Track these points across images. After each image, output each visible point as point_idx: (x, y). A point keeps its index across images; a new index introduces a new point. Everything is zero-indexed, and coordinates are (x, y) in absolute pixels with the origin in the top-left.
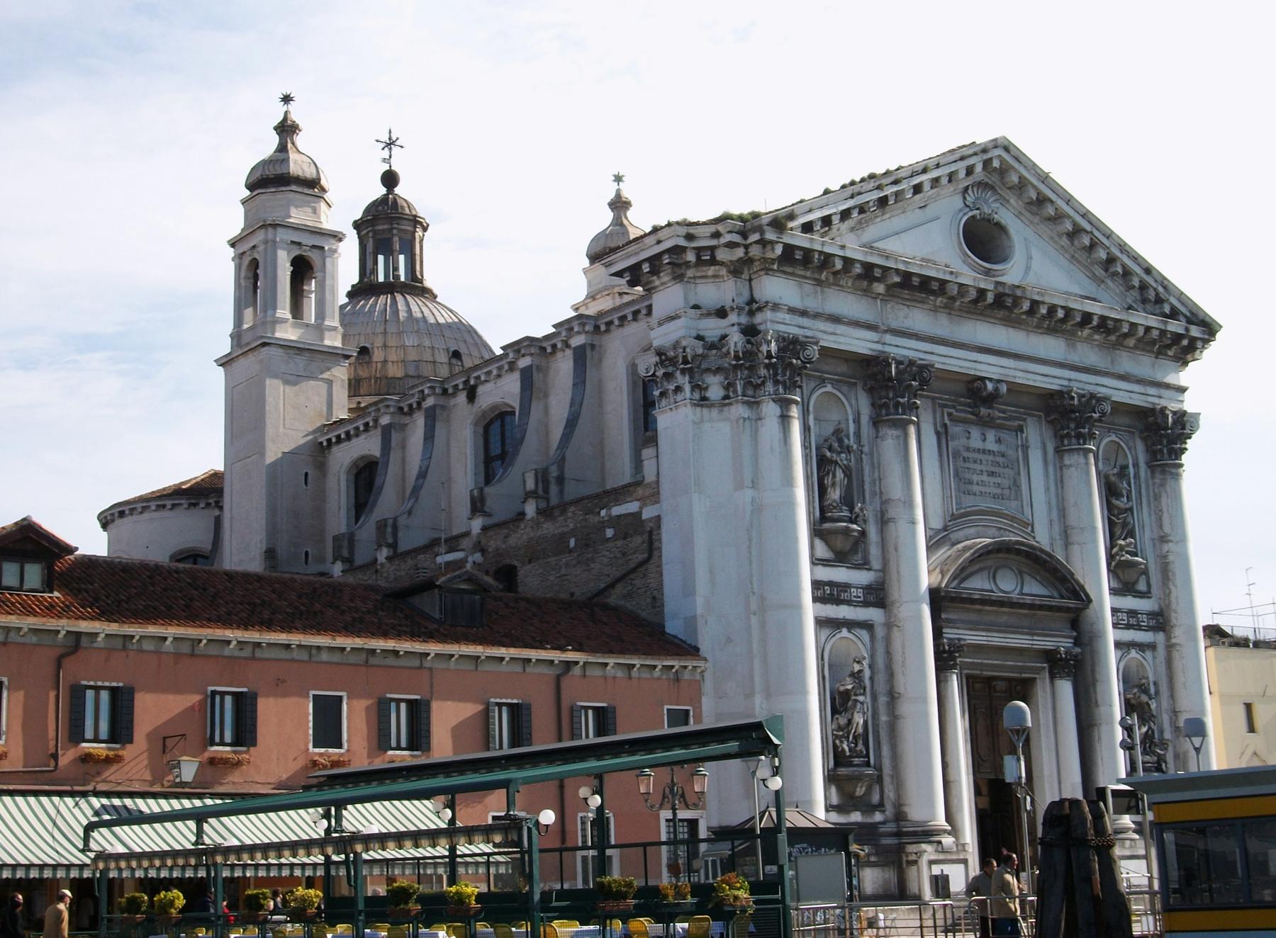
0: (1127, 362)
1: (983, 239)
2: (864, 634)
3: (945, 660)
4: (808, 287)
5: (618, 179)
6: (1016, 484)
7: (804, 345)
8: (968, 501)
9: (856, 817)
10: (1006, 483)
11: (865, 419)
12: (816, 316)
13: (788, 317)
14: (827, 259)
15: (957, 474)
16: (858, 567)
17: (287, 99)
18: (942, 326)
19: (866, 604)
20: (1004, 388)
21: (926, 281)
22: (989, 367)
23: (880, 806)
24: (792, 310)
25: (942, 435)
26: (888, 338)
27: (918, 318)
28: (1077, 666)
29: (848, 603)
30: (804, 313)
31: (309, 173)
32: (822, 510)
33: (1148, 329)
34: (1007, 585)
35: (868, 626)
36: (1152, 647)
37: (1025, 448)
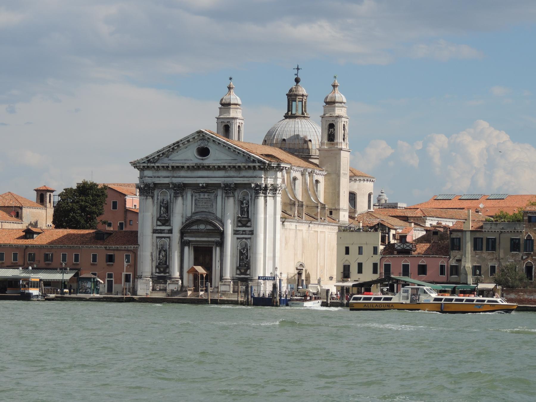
0: (244, 173)
1: (204, 152)
2: (168, 239)
3: (183, 244)
4: (154, 171)
5: (335, 77)
6: (213, 205)
7: (149, 184)
8: (198, 210)
9: (162, 274)
10: (209, 205)
11: (172, 195)
12: (155, 177)
13: (148, 179)
14: (153, 167)
15: (196, 204)
16: (168, 226)
17: (231, 79)
18: (189, 174)
19: (168, 233)
20: (204, 185)
21: (178, 167)
22: (201, 181)
23: (168, 273)
24: (149, 177)
25: (192, 196)
26: (173, 179)
27: (183, 173)
28: (221, 244)
29: (164, 233)
30: (151, 177)
31: (228, 101)
32: (160, 215)
33: (244, 166)
34: (202, 227)
35: (169, 237)
36: (250, 238)
37: (216, 196)
